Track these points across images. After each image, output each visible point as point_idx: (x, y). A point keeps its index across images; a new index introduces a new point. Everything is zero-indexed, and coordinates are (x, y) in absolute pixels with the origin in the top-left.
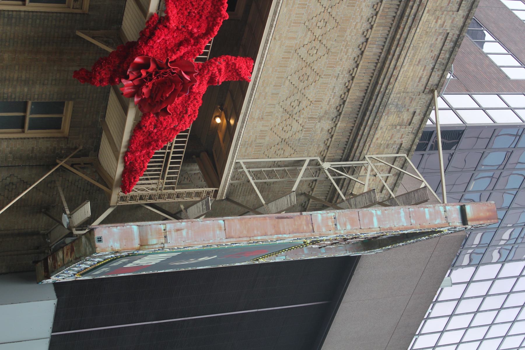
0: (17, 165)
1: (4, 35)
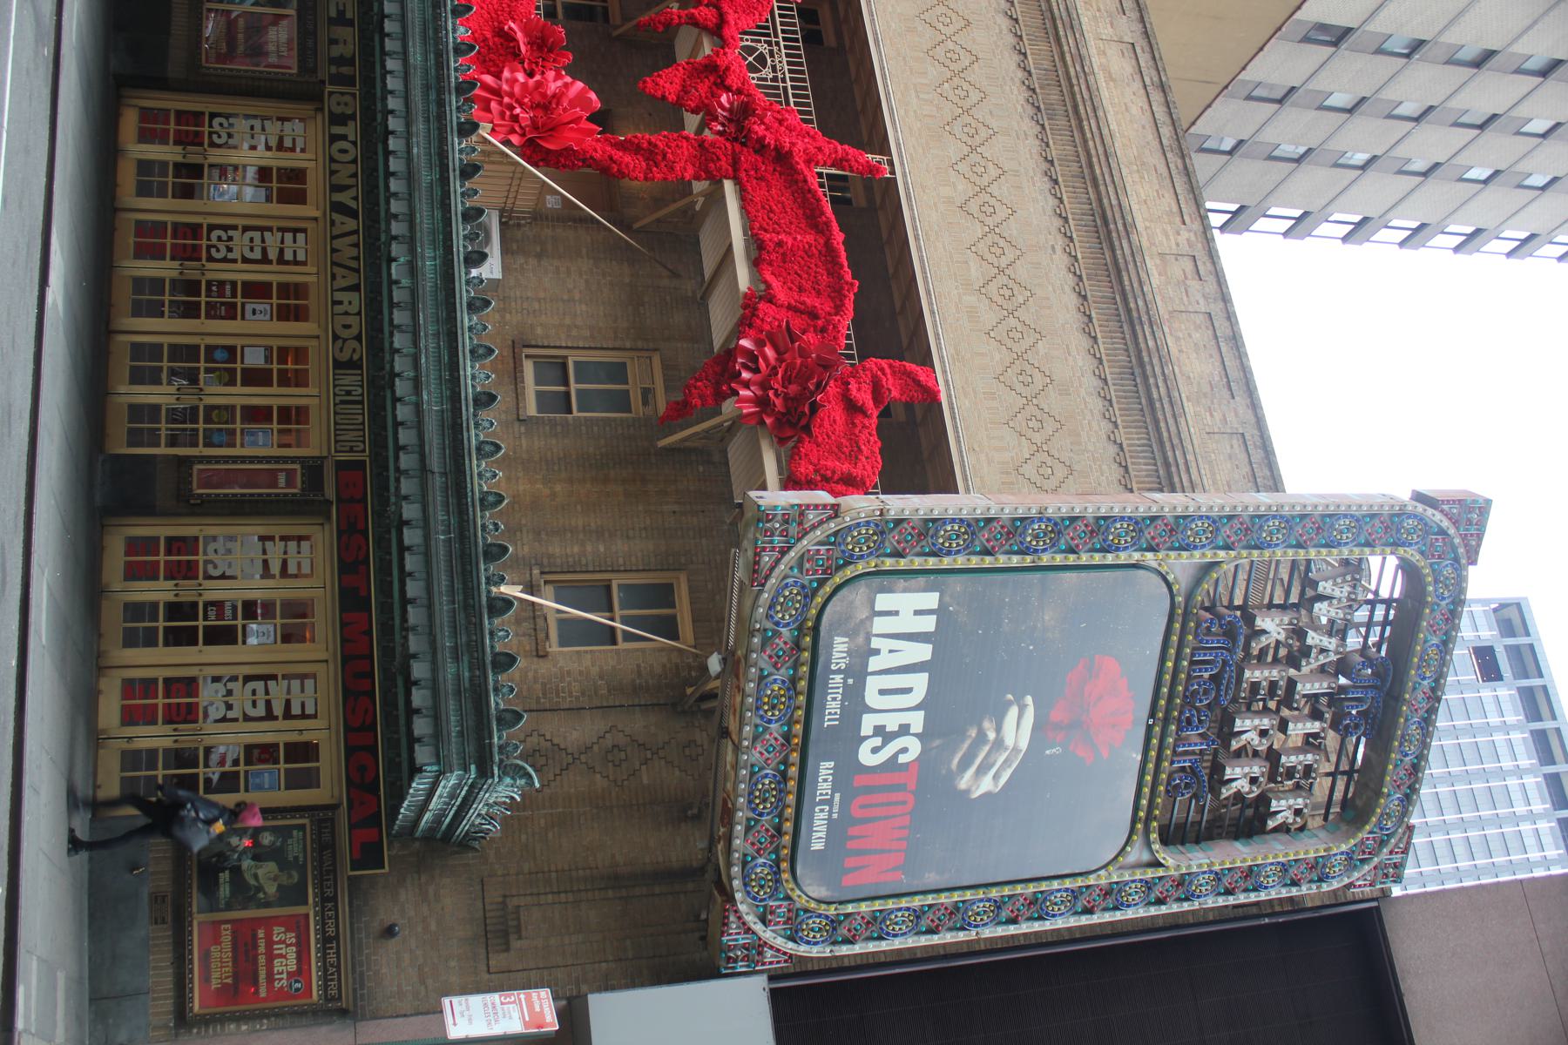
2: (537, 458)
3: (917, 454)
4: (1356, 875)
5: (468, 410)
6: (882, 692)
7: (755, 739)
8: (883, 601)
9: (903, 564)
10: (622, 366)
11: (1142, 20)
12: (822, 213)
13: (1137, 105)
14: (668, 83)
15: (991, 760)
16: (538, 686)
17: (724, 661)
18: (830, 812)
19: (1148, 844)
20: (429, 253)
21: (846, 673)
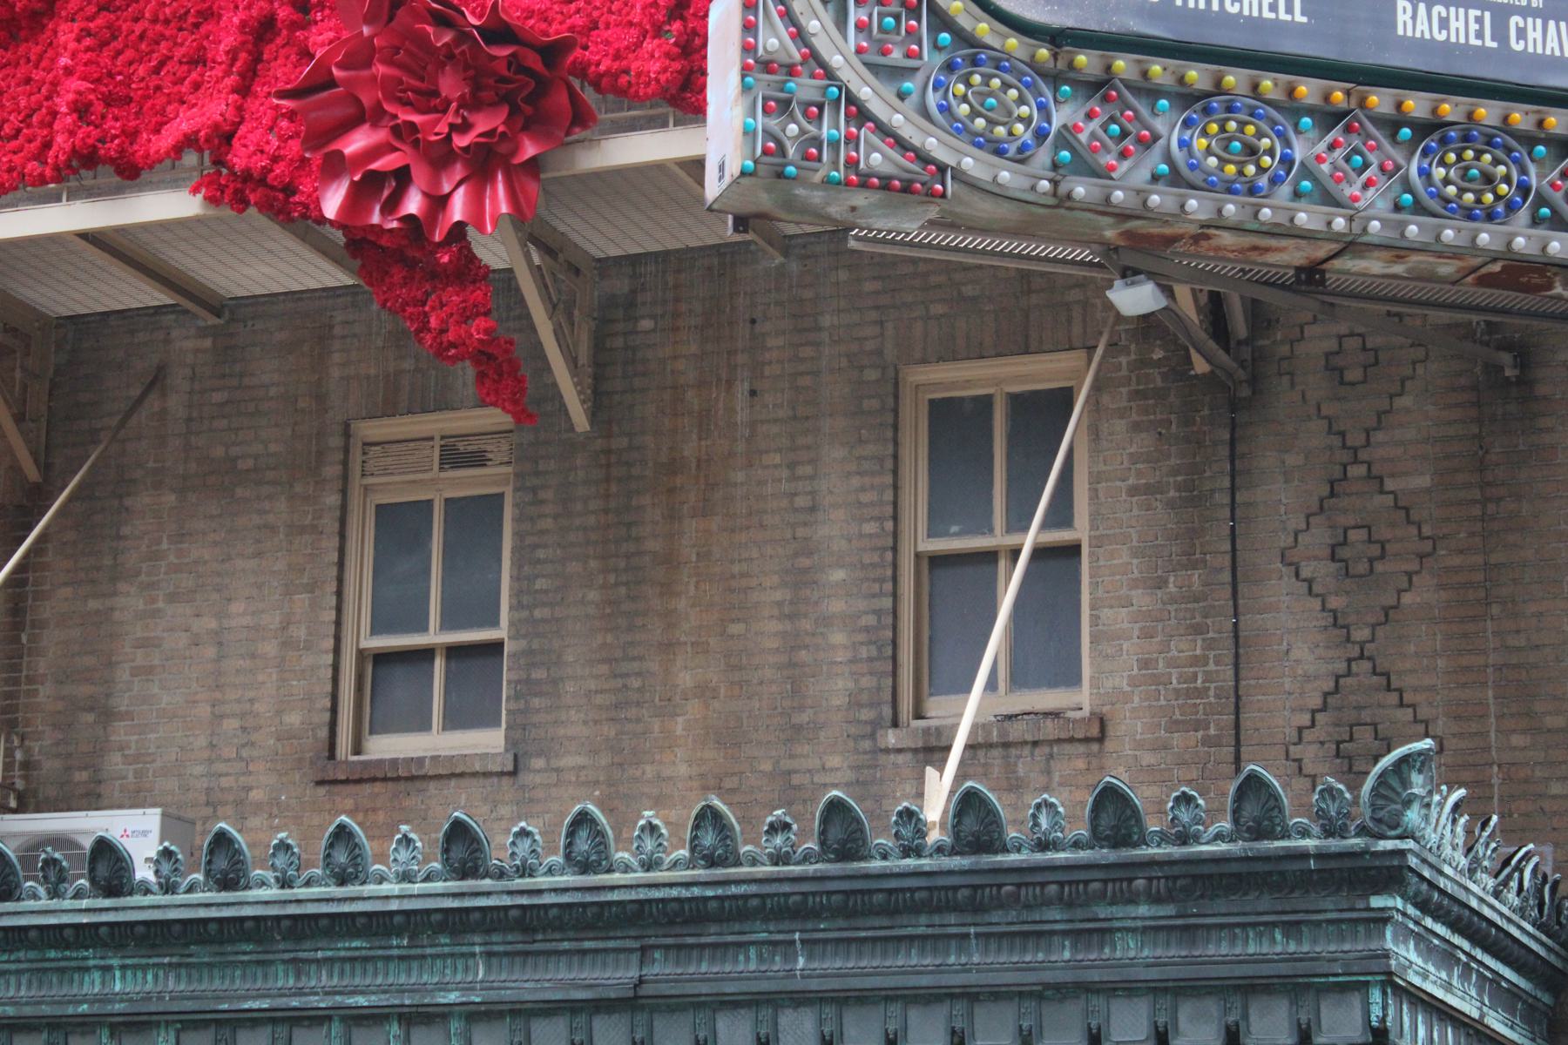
0: (1227, 546)
1: (599, 699)
2: (609, 730)
5: (488, 893)
7: (1329, 199)
10: (384, 513)
16: (1177, 739)
17: (1129, 273)
20: (93, 984)
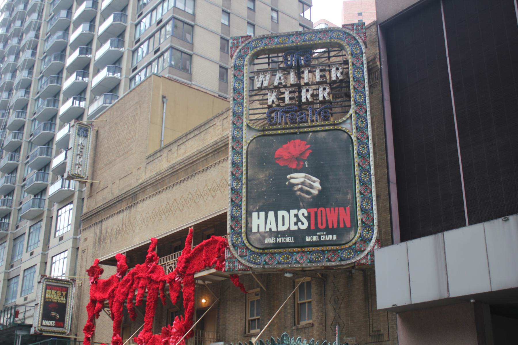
3: (216, 225)
4: (360, 41)
6: (283, 225)
7: (299, 263)
8: (255, 230)
9: (244, 225)
10: (251, 302)
11: (172, 144)
12: (198, 248)
13: (190, 143)
14: (173, 296)
15: (308, 185)
17: (286, 273)
18: (323, 235)
19: (344, 121)
21: (276, 237)
